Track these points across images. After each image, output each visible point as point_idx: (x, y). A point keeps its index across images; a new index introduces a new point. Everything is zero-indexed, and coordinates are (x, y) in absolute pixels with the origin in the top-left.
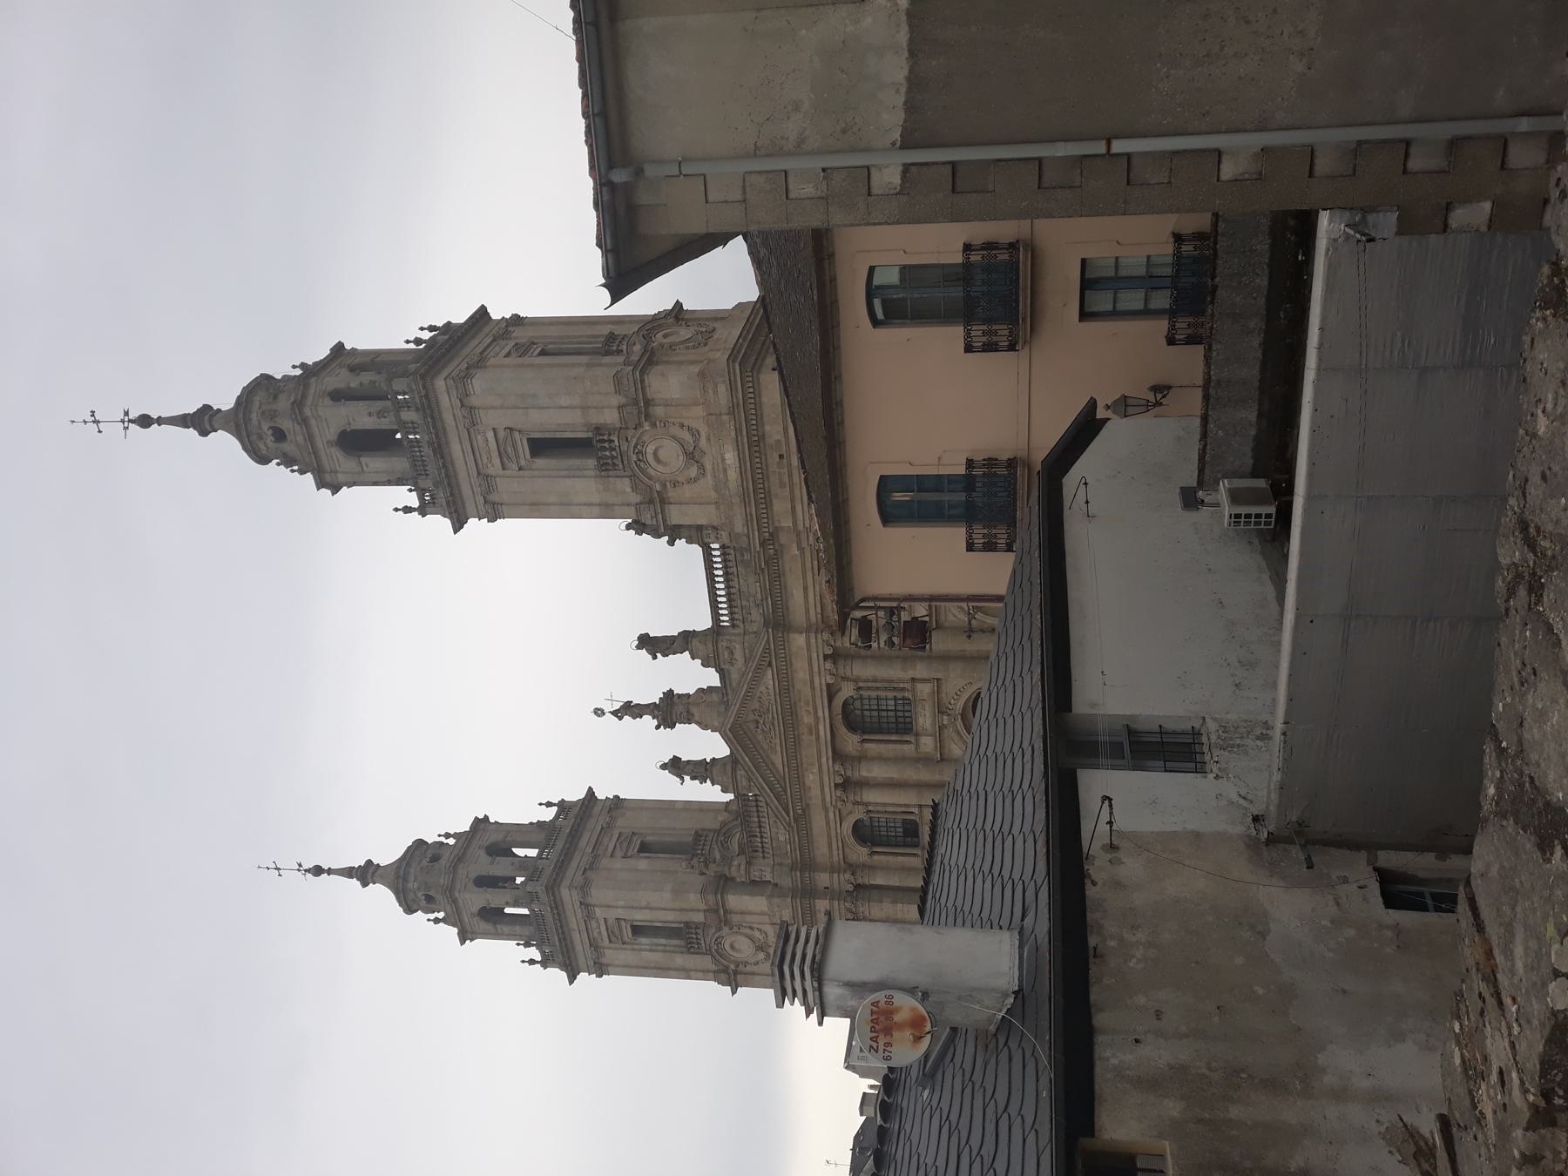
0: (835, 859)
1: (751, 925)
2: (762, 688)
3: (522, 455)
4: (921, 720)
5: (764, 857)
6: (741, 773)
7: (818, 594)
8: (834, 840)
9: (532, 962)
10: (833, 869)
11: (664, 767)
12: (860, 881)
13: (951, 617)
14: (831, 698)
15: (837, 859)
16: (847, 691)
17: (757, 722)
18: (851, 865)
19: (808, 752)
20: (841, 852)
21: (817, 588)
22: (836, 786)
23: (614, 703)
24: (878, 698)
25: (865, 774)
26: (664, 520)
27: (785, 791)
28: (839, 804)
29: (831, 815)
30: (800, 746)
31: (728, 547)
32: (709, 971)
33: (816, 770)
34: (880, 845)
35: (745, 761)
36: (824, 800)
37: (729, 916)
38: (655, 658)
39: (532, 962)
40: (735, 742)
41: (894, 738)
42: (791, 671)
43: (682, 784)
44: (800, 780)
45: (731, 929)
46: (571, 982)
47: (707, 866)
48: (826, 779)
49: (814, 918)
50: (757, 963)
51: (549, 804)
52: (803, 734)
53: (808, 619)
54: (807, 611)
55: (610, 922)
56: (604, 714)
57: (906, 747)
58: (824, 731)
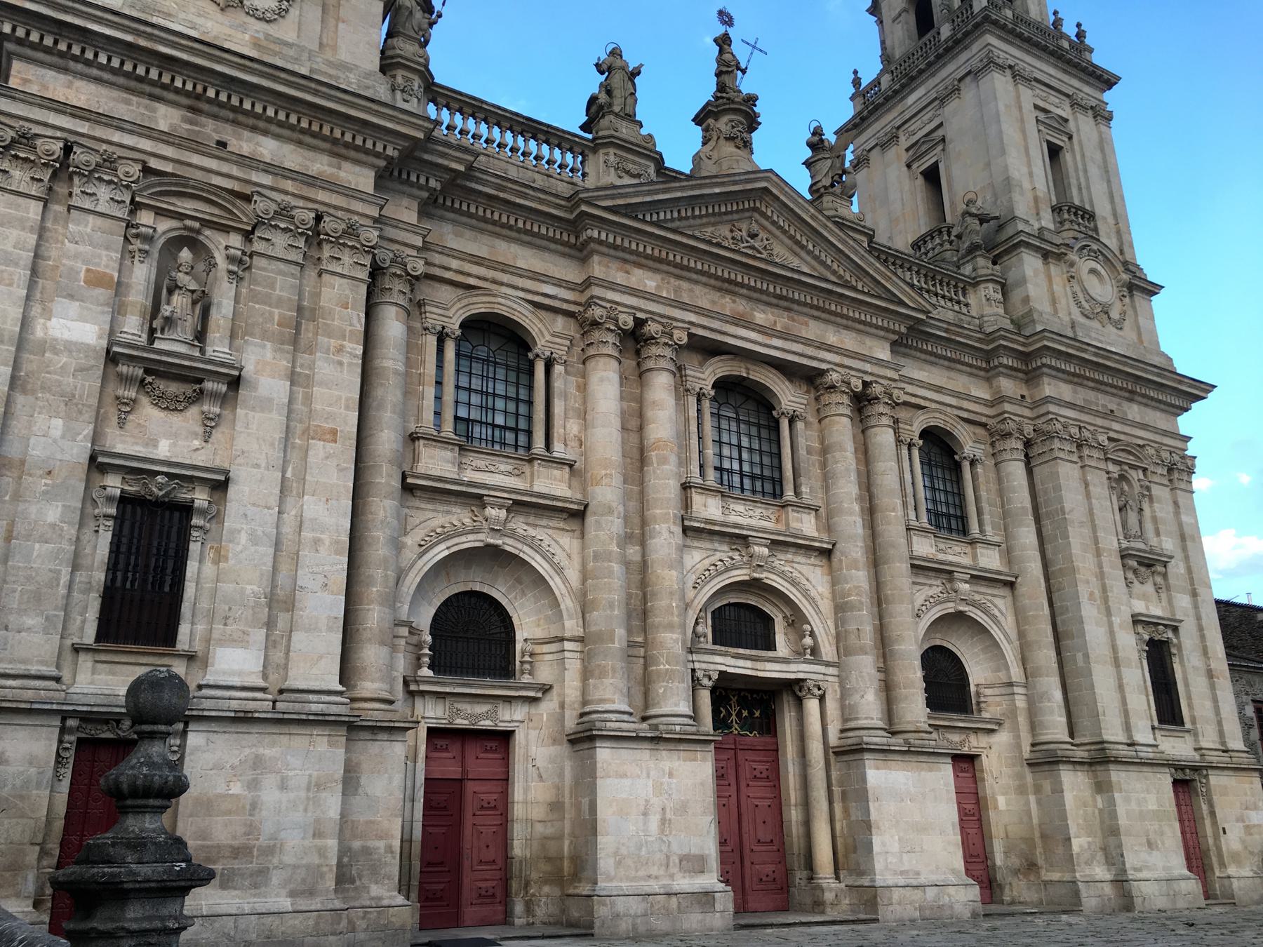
4: (740, 508)
8: (490, 274)
11: (616, 53)
15: (437, 262)
16: (788, 396)
19: (704, 297)
20: (448, 275)
21: (934, 406)
22: (640, 323)
26: (1028, 245)
27: (657, 224)
30: (714, 287)
36: (613, 286)
40: (749, 186)
42: (839, 325)
49: (326, 146)
52: (734, 302)
56: (724, 22)
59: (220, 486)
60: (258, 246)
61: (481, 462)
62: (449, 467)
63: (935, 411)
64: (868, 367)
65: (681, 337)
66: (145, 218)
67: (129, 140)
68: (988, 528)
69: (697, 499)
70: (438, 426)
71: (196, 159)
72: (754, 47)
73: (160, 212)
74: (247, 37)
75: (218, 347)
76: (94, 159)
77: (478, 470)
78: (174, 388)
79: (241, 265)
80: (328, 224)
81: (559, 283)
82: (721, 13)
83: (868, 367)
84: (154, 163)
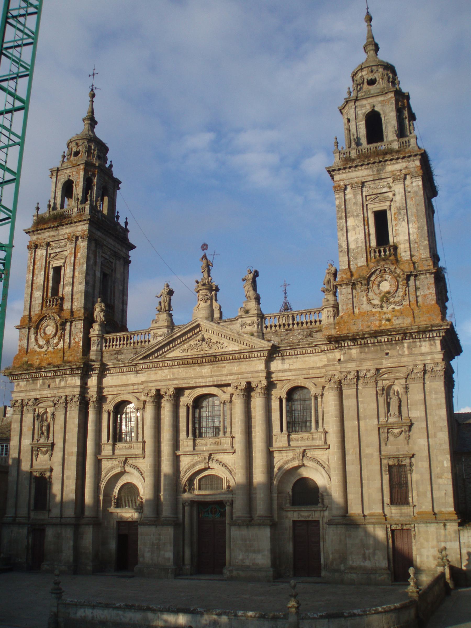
1: (63, 338)
3: (374, 206)
5: (106, 346)
9: (38, 209)
10: (100, 389)
23: (212, 256)
24: (219, 416)
28: (147, 392)
31: (320, 323)
32: (30, 312)
39: (38, 209)
43: (157, 297)
46: (24, 230)
48: (163, 383)
50: (36, 340)
51: (126, 223)
55: (65, 253)
56: (203, 250)
57: (185, 433)
59: (51, 470)
64: (250, 375)
65: (171, 391)
72: (214, 255)
77: (120, 449)
79: (53, 415)
82: (202, 247)
83: (250, 375)
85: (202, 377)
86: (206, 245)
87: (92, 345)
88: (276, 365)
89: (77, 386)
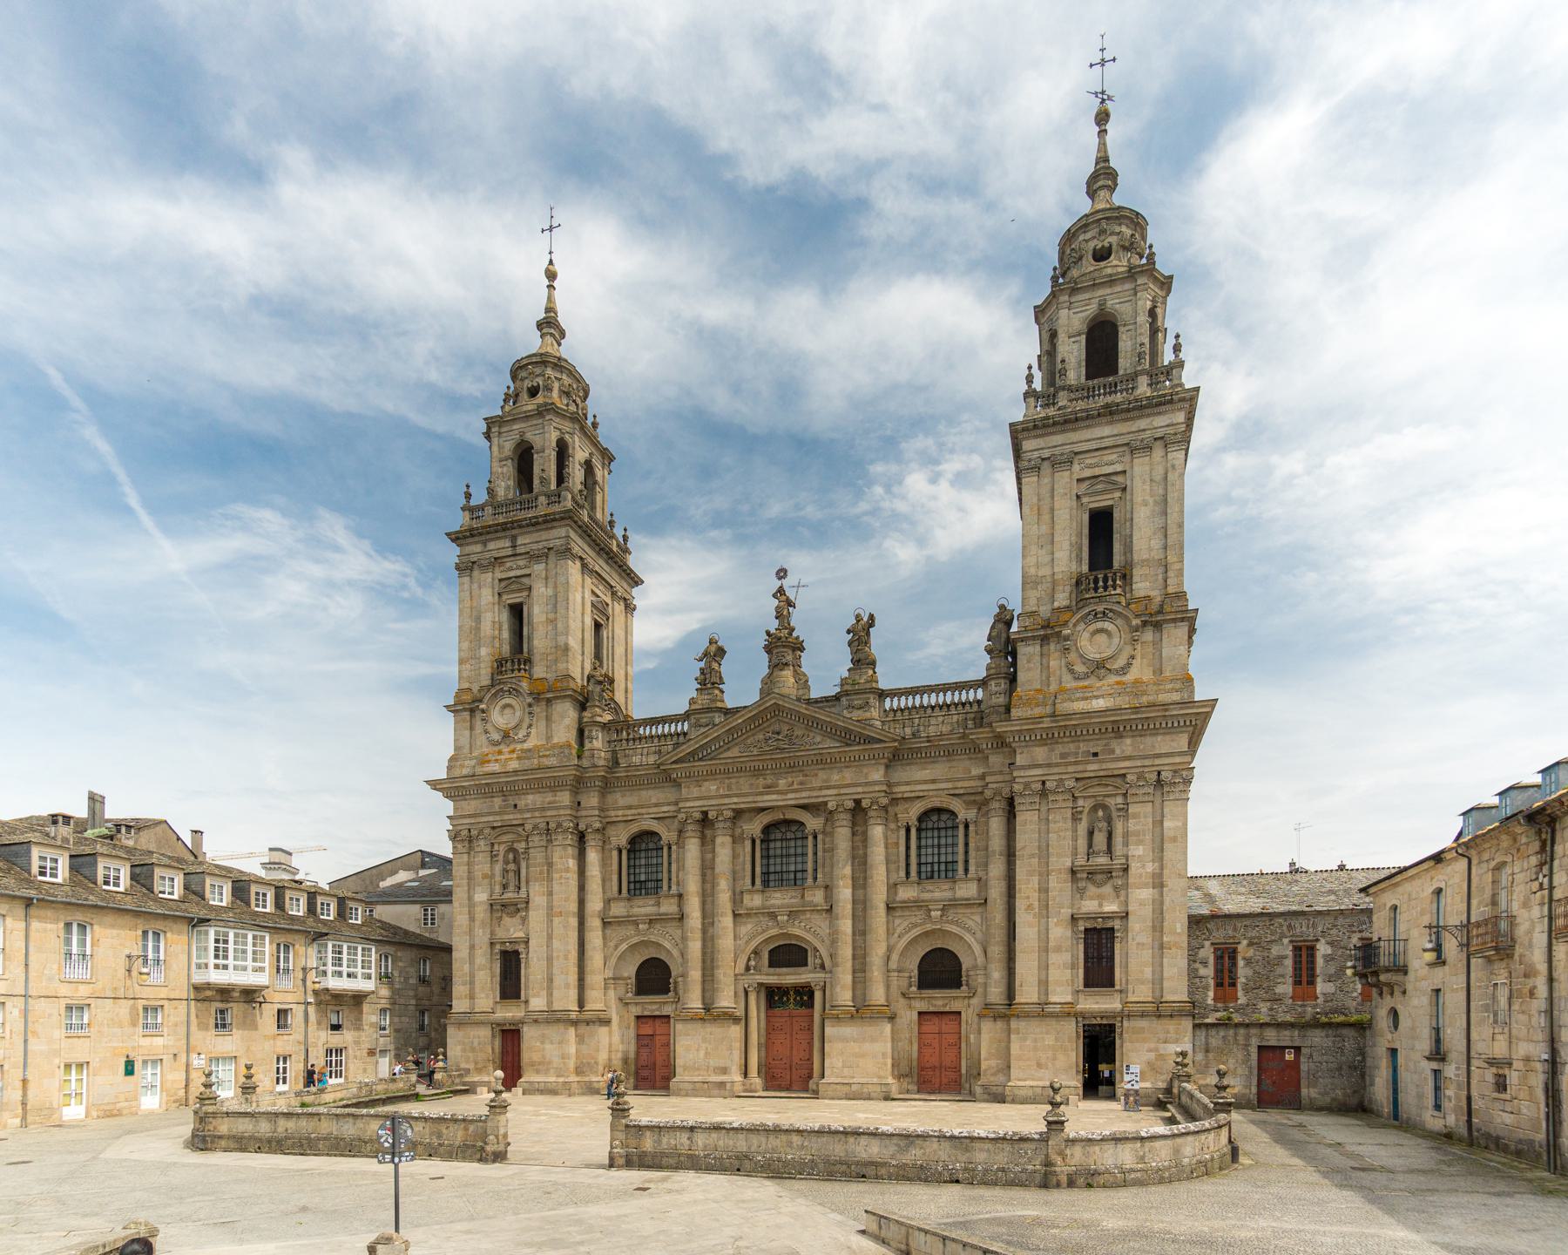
0: (613, 813)
2: (818, 739)
6: (718, 718)
7: (925, 794)
12: (589, 837)
13: (897, 921)
14: (804, 807)
16: (813, 823)
17: (778, 733)
18: (604, 829)
19: (744, 784)
20: (619, 819)
21: (931, 793)
22: (705, 813)
23: (795, 589)
25: (719, 840)
28: (683, 816)
29: (665, 809)
33: (721, 792)
34: (629, 859)
35: (737, 719)
37: (544, 703)
38: (849, 632)
40: (762, 708)
41: (758, 870)
44: (712, 775)
45: (530, 705)
47: (600, 683)
52: (765, 779)
53: (898, 784)
54: (908, 783)
56: (780, 578)
57: (748, 881)
58: (770, 799)
60: (530, 844)
61: (641, 903)
62: (623, 910)
63: (932, 797)
64: (860, 789)
65: (729, 814)
66: (496, 847)
67: (485, 819)
68: (972, 869)
69: (746, 898)
70: (620, 892)
71: (506, 817)
73: (499, 843)
74: (515, 756)
75: (523, 889)
76: (476, 832)
77: (639, 907)
78: (512, 908)
80: (552, 825)
81: (669, 804)
82: (778, 573)
83: (860, 789)
84: (495, 825)
85: (778, 792)
86: (785, 571)
87: (586, 741)
88: (900, 774)
89: (565, 807)
